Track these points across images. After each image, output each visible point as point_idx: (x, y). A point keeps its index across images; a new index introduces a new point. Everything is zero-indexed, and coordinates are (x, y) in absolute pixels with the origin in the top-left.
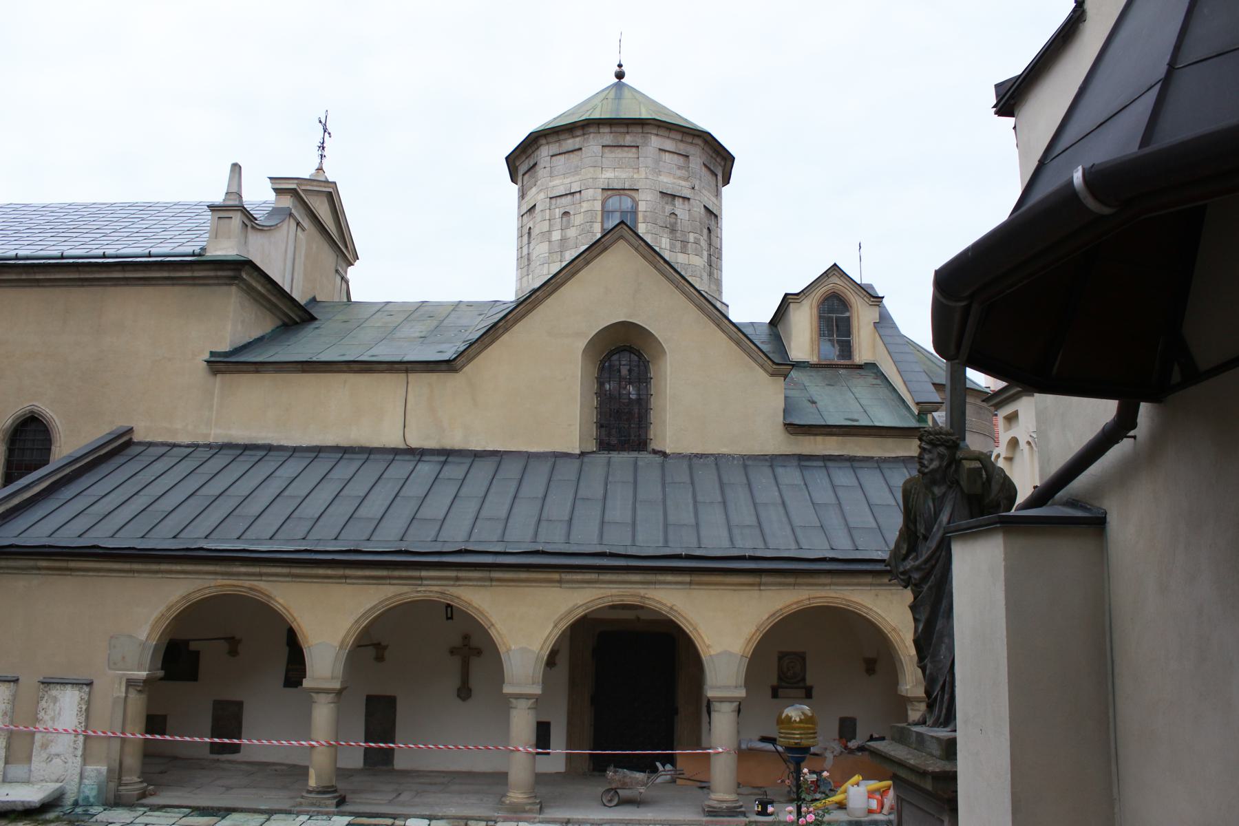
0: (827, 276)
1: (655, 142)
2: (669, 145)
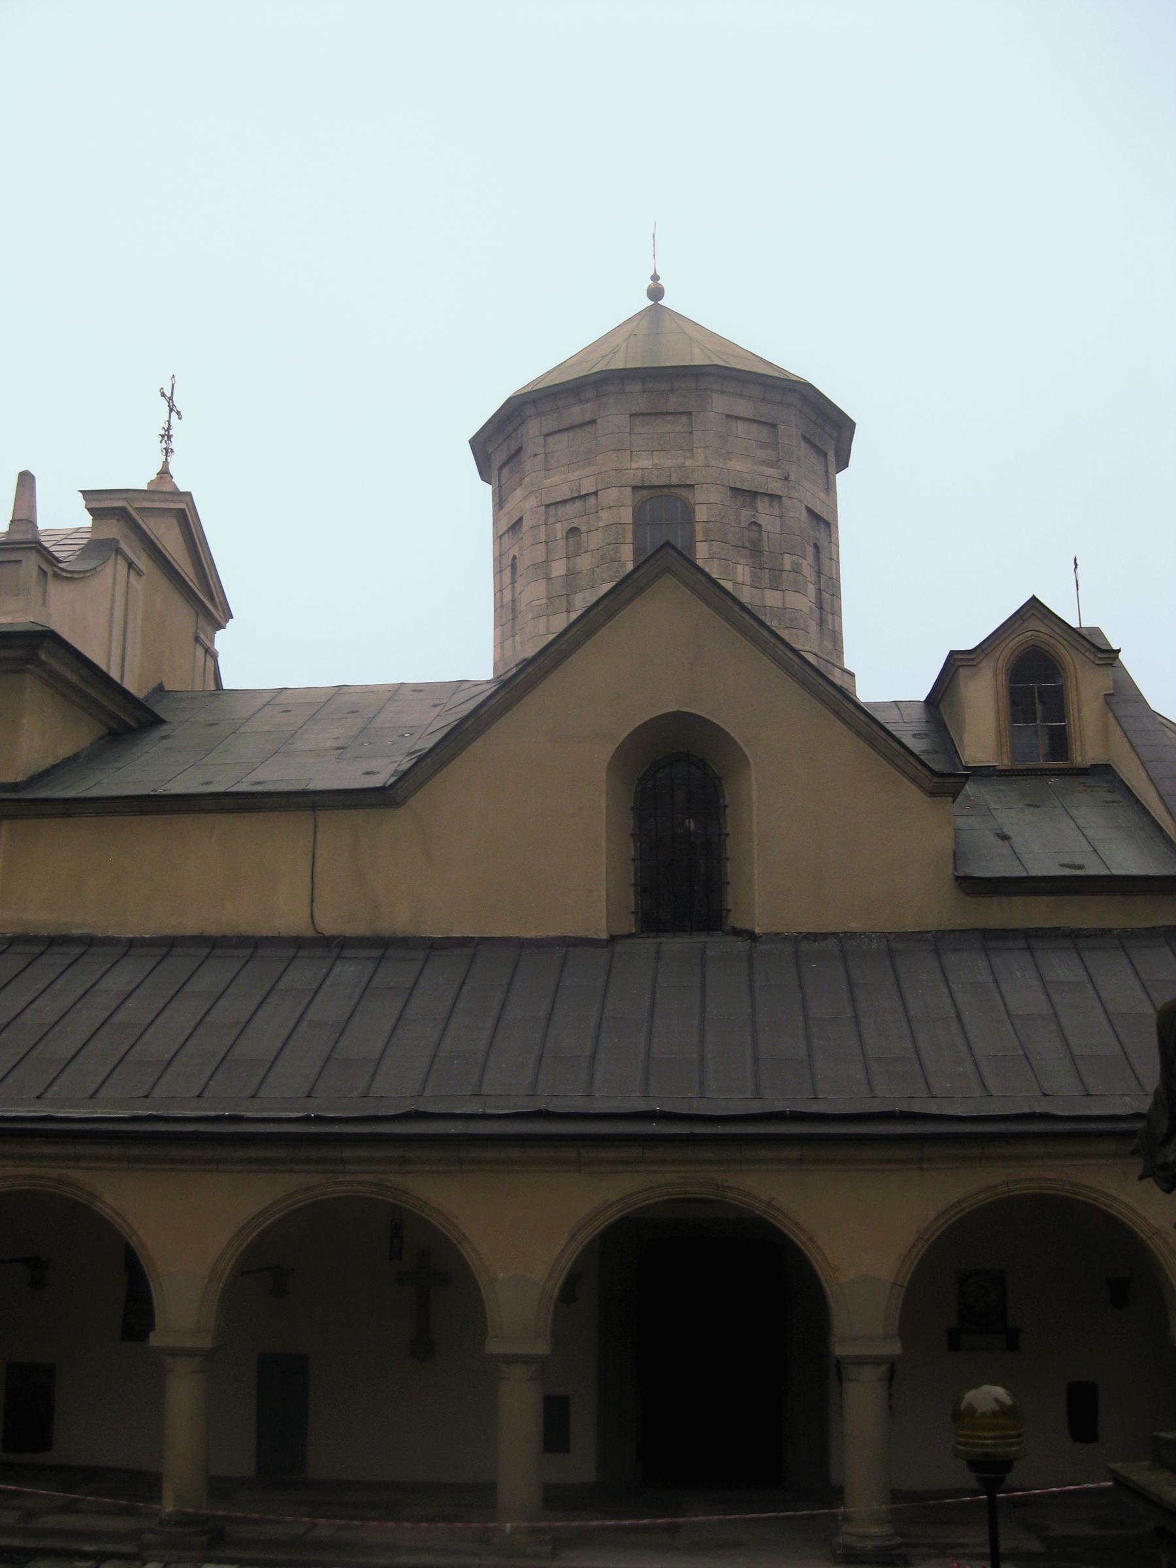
0: (1021, 617)
1: (719, 404)
2: (742, 407)
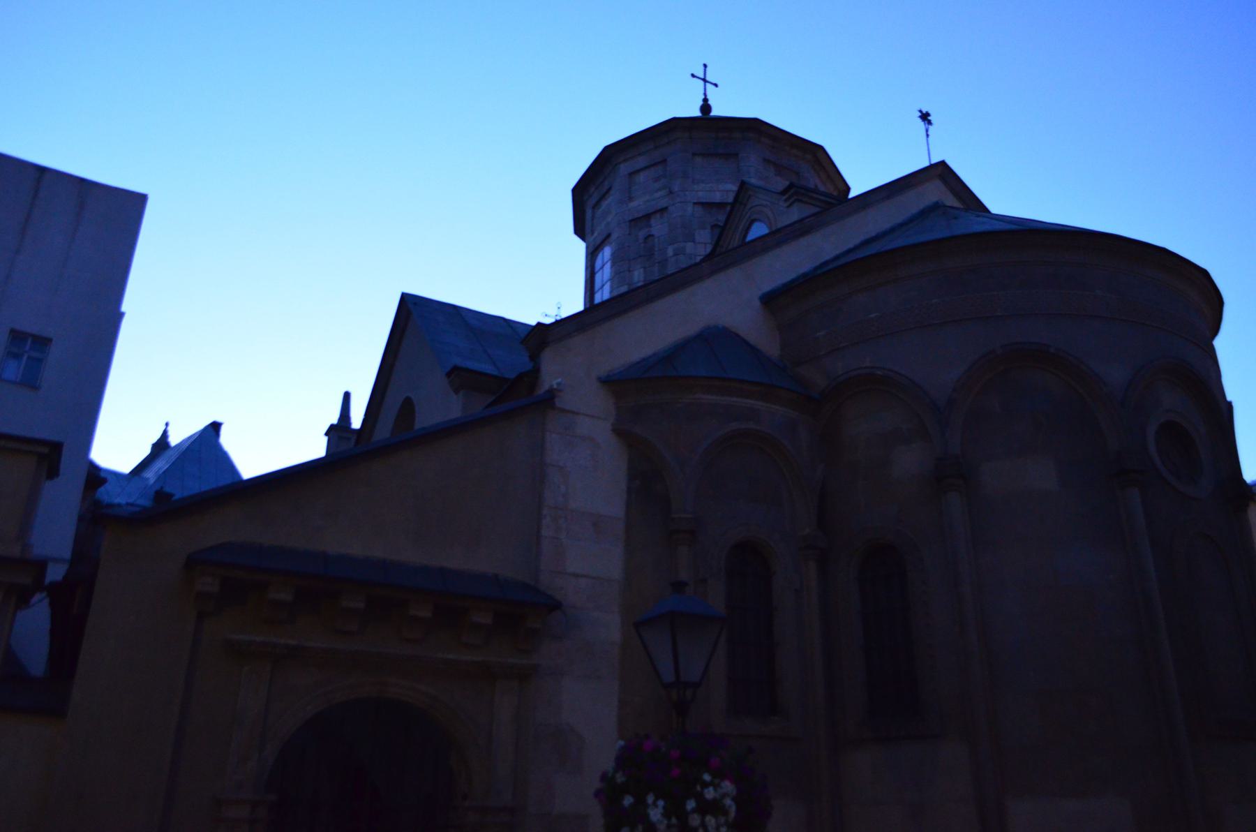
1: (624, 168)
2: (641, 162)
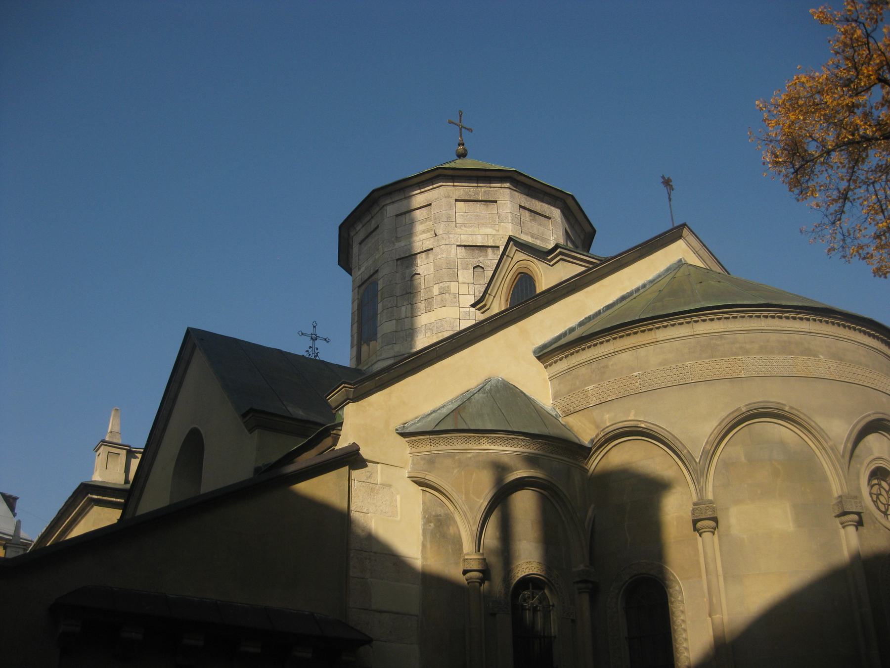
0: (508, 256)
